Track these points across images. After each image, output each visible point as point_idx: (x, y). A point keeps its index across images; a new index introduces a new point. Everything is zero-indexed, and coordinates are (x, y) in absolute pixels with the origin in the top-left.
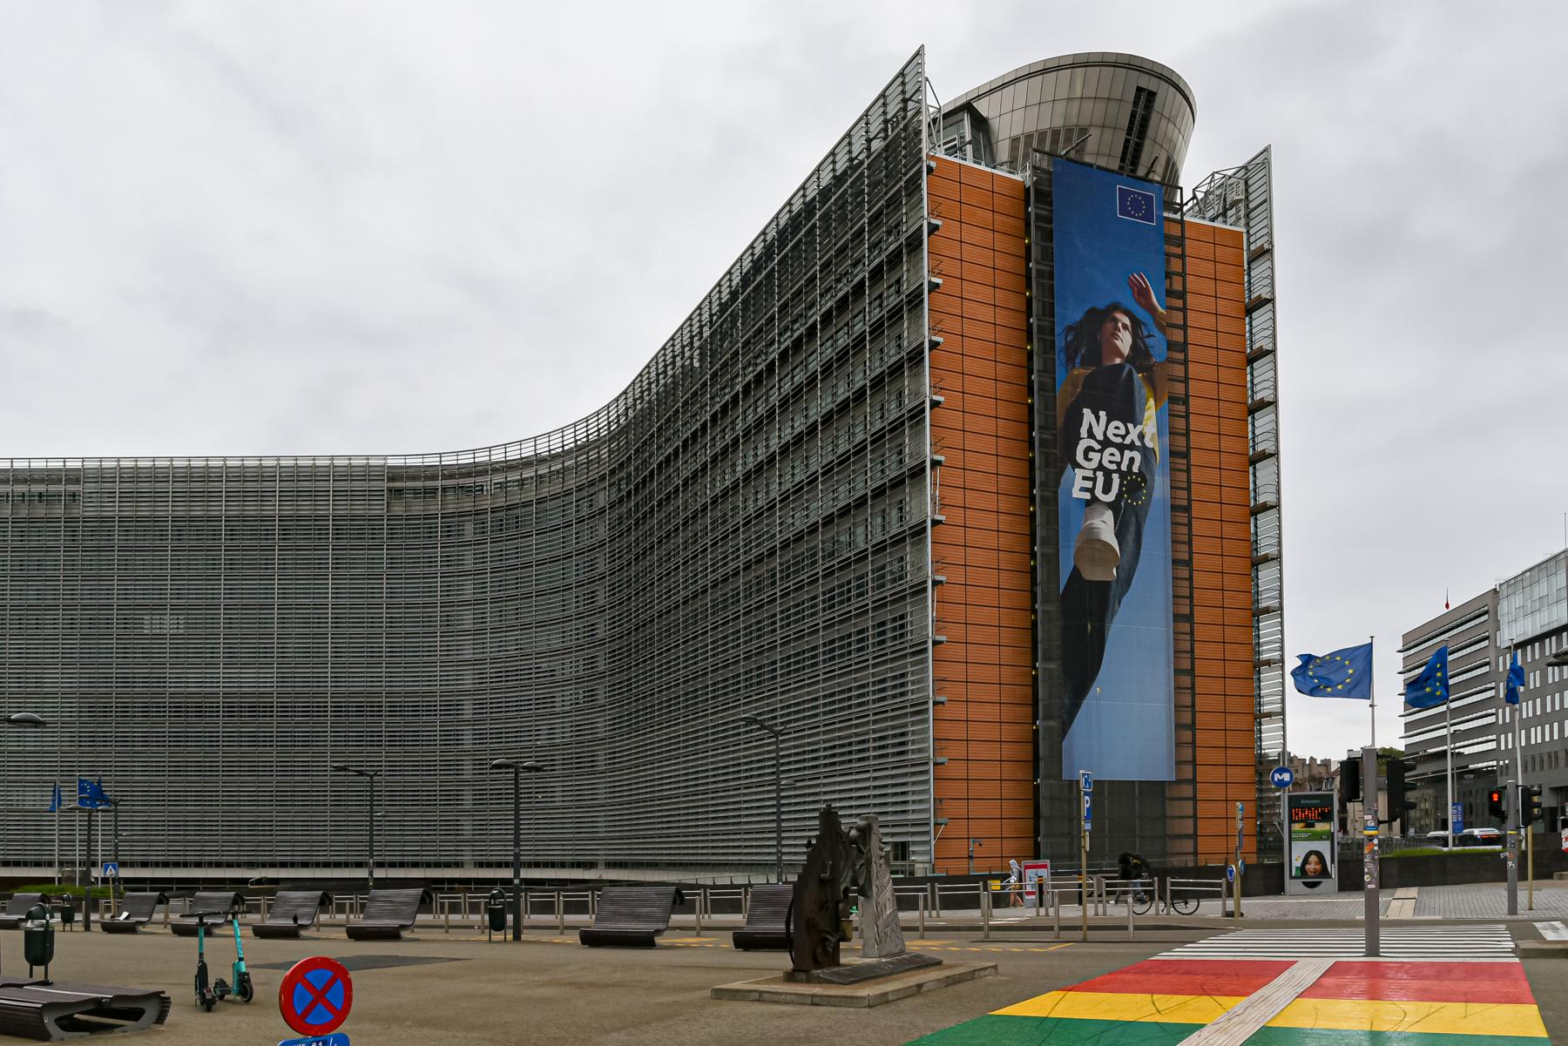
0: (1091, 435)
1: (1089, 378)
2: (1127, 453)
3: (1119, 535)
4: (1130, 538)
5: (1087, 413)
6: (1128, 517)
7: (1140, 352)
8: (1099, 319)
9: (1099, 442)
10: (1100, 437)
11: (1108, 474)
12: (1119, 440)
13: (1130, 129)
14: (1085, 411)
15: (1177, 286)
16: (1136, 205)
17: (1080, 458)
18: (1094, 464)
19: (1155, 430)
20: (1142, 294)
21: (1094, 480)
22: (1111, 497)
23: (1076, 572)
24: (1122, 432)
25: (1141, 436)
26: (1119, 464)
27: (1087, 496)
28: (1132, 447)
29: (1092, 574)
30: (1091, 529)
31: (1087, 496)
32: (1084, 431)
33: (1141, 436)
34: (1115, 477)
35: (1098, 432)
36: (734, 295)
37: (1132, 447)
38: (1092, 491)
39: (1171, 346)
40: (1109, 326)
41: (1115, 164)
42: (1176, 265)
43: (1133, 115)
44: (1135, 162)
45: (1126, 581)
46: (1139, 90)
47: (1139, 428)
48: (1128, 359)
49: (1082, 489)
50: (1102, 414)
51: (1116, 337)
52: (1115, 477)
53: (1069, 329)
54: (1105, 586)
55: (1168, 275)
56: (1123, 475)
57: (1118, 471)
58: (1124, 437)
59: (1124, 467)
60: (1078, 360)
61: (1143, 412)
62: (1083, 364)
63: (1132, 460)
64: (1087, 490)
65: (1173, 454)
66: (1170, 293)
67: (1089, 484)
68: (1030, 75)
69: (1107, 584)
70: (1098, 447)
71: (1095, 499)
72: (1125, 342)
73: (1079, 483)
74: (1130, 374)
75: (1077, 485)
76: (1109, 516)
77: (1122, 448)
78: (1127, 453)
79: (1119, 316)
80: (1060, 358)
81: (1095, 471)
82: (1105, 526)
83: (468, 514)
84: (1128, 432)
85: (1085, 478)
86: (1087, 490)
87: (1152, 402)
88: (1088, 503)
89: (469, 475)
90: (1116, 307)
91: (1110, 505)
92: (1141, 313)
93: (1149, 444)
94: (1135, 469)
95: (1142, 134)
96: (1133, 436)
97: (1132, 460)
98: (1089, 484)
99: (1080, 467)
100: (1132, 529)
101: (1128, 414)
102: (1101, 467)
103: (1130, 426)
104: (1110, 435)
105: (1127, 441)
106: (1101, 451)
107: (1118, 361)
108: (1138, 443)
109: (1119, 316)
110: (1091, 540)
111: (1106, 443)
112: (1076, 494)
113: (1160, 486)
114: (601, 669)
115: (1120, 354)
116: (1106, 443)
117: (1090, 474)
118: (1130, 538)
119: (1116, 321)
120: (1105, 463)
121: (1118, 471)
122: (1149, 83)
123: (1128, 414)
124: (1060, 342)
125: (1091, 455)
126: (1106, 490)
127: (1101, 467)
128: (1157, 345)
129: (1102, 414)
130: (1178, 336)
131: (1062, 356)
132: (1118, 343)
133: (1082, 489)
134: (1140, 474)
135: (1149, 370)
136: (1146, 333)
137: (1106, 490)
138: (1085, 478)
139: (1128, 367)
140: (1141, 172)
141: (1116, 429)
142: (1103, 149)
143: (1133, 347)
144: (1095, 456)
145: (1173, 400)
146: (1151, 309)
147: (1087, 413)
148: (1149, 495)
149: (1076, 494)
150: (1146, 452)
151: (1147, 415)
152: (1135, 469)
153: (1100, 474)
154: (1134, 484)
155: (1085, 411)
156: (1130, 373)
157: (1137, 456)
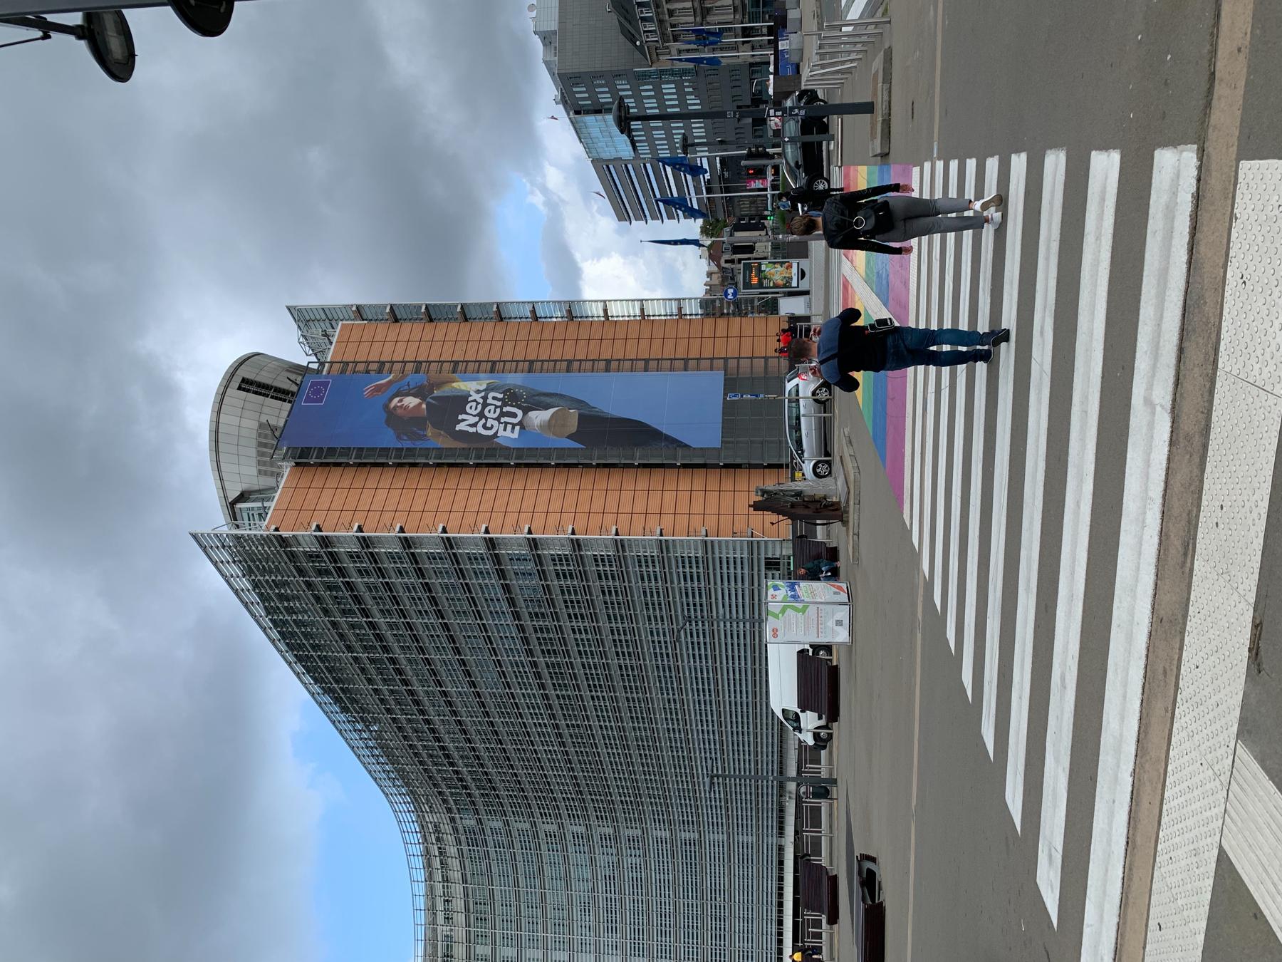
0: (475, 425)
2: (490, 401)
3: (546, 407)
4: (548, 400)
6: (533, 402)
7: (419, 392)
8: (394, 419)
10: (477, 419)
11: (503, 414)
12: (480, 407)
13: (264, 395)
15: (374, 367)
16: (317, 392)
17: (490, 433)
20: (378, 389)
21: (506, 423)
22: (520, 413)
25: (478, 392)
26: (497, 407)
27: (517, 428)
28: (485, 398)
29: (573, 426)
30: (541, 427)
31: (517, 428)
32: (472, 430)
33: (478, 392)
34: (505, 409)
35: (473, 420)
36: (327, 691)
38: (514, 425)
39: (417, 371)
40: (399, 411)
41: (287, 406)
42: (361, 367)
43: (256, 393)
44: (286, 392)
45: (579, 403)
46: (240, 388)
48: (423, 399)
50: (460, 417)
51: (407, 407)
52: (505, 409)
53: (399, 438)
54: (582, 418)
55: (368, 372)
56: (505, 404)
57: (501, 407)
59: (499, 404)
62: (425, 429)
63: (494, 398)
64: (513, 428)
65: (492, 371)
66: (380, 371)
67: (509, 427)
68: (218, 461)
70: (483, 421)
72: (411, 401)
73: (508, 433)
75: (509, 436)
77: (485, 405)
82: (539, 417)
83: (468, 949)
86: (513, 428)
87: (455, 385)
89: (435, 947)
90: (386, 406)
91: (525, 413)
92: (393, 390)
93: (484, 387)
94: (501, 396)
95: (268, 387)
96: (478, 397)
97: (494, 398)
98: (509, 427)
100: (543, 399)
101: (461, 401)
102: (498, 419)
105: (481, 401)
106: (487, 418)
107: (424, 406)
110: (550, 425)
111: (481, 415)
112: (515, 435)
113: (514, 379)
114: (611, 831)
115: (420, 404)
116: (481, 415)
117: (502, 426)
118: (548, 400)
119: (396, 407)
121: (501, 407)
122: (236, 382)
123: (461, 401)
124: (407, 444)
125: (489, 425)
126: (514, 415)
127: (498, 419)
128: (414, 379)
129: (460, 417)
130: (410, 367)
134: (503, 392)
135: (432, 386)
137: (514, 415)
140: (294, 388)
142: (277, 413)
143: (415, 396)
145: (454, 371)
148: (520, 387)
150: (489, 389)
152: (501, 396)
153: (503, 420)
154: (511, 397)
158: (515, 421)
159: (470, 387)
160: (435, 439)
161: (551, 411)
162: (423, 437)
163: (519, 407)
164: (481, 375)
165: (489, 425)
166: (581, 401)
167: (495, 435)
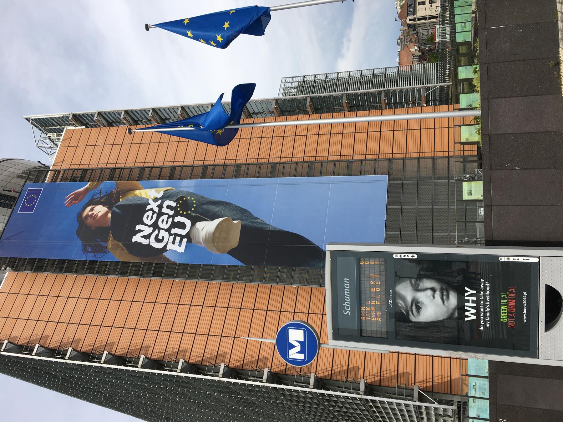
0: (147, 237)
1: (115, 238)
2: (165, 210)
3: (212, 218)
4: (215, 209)
5: (137, 238)
9: (154, 231)
10: (152, 228)
14: (133, 240)
17: (160, 246)
18: (166, 234)
19: (154, 190)
20: (77, 197)
21: (176, 235)
22: (188, 223)
23: (232, 253)
24: (150, 213)
26: (169, 216)
27: (185, 240)
28: (160, 207)
29: (234, 239)
30: (206, 240)
31: (185, 240)
32: (145, 242)
33: (156, 200)
34: (178, 219)
35: (148, 231)
37: (160, 207)
38: (182, 237)
40: (89, 220)
45: (242, 213)
47: (151, 201)
48: (110, 208)
49: (180, 245)
50: (138, 227)
52: (177, 219)
53: (85, 250)
54: (244, 229)
56: (177, 214)
57: (173, 217)
58: (154, 212)
59: (171, 213)
60: (103, 244)
61: (142, 198)
62: (106, 240)
63: (169, 207)
64: (181, 241)
67: (178, 239)
69: (243, 228)
71: (188, 236)
72: (100, 210)
74: (118, 207)
75: (177, 249)
76: (200, 225)
77: (160, 214)
78: (165, 210)
79: (85, 214)
80: (101, 258)
81: (170, 235)
82: (206, 228)
84: (151, 209)
85: (173, 243)
86: (181, 241)
87: (137, 192)
88: (189, 241)
90: (80, 214)
91: (193, 224)
92: (86, 200)
94: (174, 204)
96: (154, 206)
97: (169, 207)
98: (178, 239)
99: (166, 246)
100: (210, 207)
101: (140, 208)
102: (168, 230)
103: (148, 207)
104: (150, 222)
105: (156, 210)
106: (159, 229)
107: (109, 215)
108: (159, 202)
109: (85, 214)
111: (155, 226)
112: (182, 249)
113: (187, 186)
115: (106, 213)
116: (155, 226)
117: (172, 238)
118: (215, 209)
119: (87, 216)
120: (167, 227)
121: (173, 217)
123: (140, 208)
124: (90, 257)
125: (160, 237)
126: (182, 226)
127: (168, 230)
128: (106, 186)
129: (138, 227)
131: (98, 256)
132: (100, 214)
133: (180, 245)
134: (177, 201)
136: (98, 196)
137: (182, 226)
138: (173, 243)
139: (115, 209)
140: (17, 195)
141: (148, 218)
143: (104, 205)
144: (163, 233)
146: (87, 190)
147: (137, 238)
148: (192, 194)
149: (182, 249)
150: (164, 198)
151: (144, 196)
153: (174, 231)
155: (133, 240)
156: (118, 207)
157: (167, 203)
158: (183, 232)
159: (149, 193)
160: (116, 253)
161: (217, 221)
162: (103, 250)
163: (188, 217)
164: (161, 182)
165: (160, 237)
166: (244, 211)
167: (164, 249)
